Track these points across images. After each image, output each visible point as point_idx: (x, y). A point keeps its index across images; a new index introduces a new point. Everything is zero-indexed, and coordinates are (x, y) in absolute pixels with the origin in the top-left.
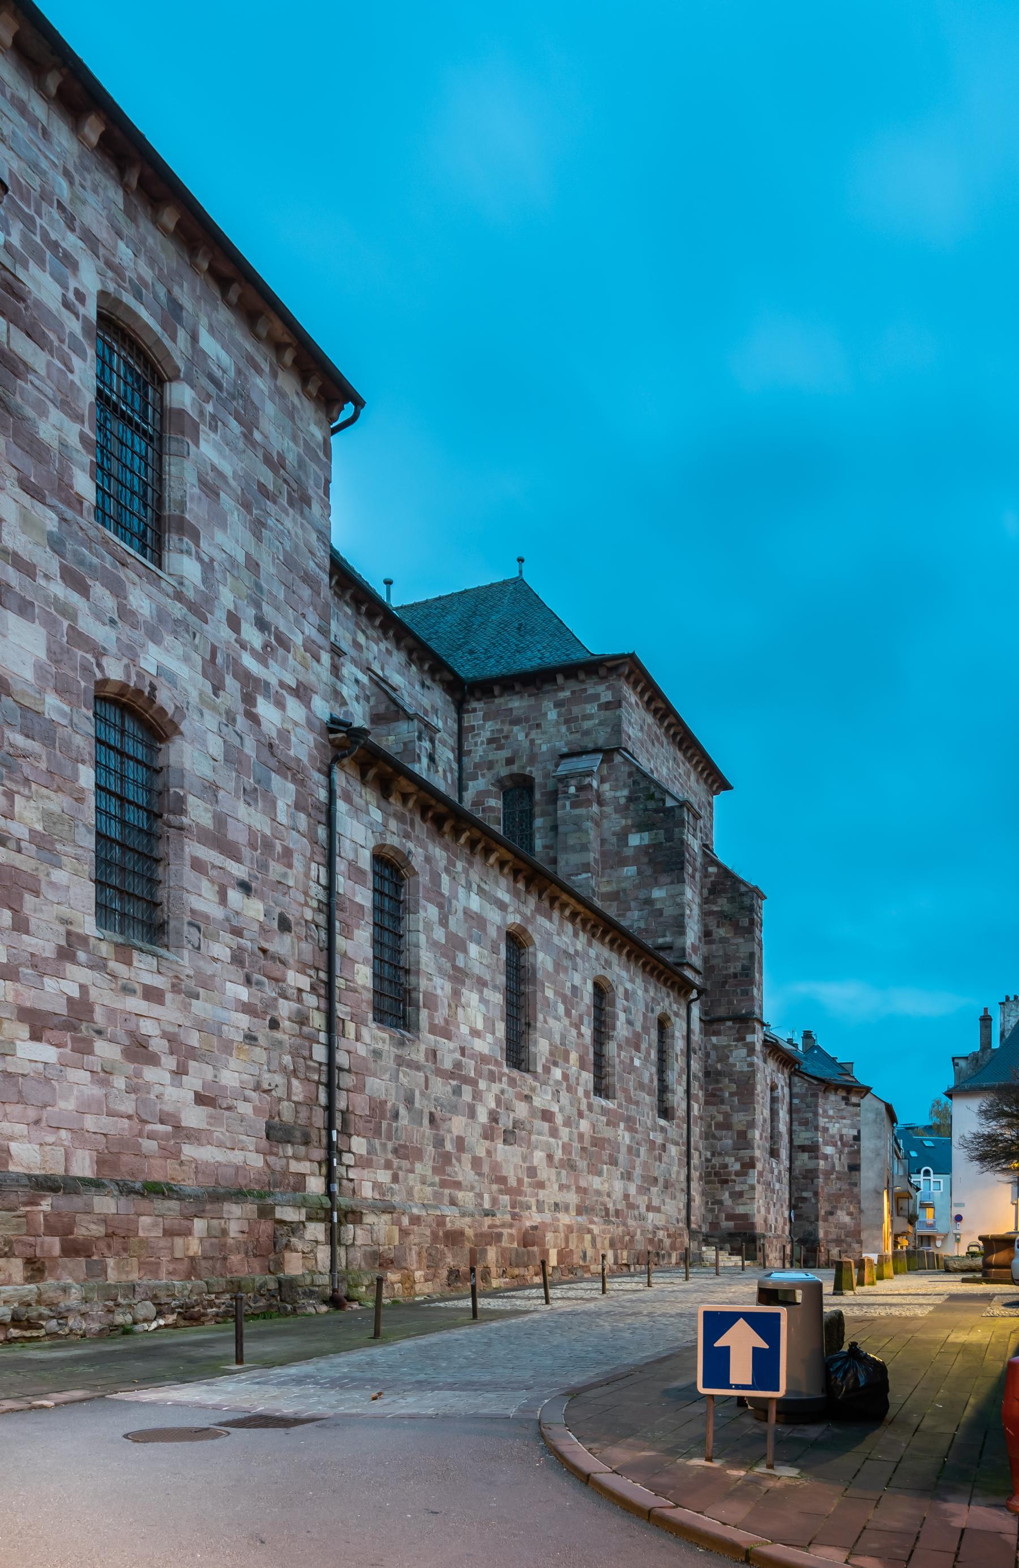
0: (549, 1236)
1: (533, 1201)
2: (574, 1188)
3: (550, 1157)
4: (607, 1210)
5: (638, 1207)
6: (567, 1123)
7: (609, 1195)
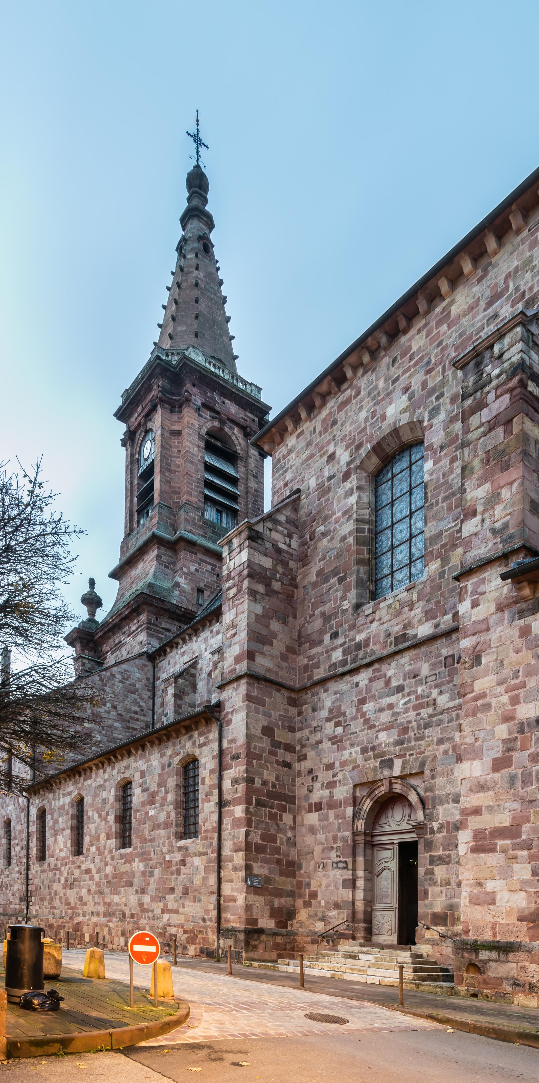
0: (85, 927)
1: (81, 912)
2: (102, 904)
3: (89, 890)
4: (124, 915)
5: (152, 911)
6: (99, 871)
7: (126, 905)
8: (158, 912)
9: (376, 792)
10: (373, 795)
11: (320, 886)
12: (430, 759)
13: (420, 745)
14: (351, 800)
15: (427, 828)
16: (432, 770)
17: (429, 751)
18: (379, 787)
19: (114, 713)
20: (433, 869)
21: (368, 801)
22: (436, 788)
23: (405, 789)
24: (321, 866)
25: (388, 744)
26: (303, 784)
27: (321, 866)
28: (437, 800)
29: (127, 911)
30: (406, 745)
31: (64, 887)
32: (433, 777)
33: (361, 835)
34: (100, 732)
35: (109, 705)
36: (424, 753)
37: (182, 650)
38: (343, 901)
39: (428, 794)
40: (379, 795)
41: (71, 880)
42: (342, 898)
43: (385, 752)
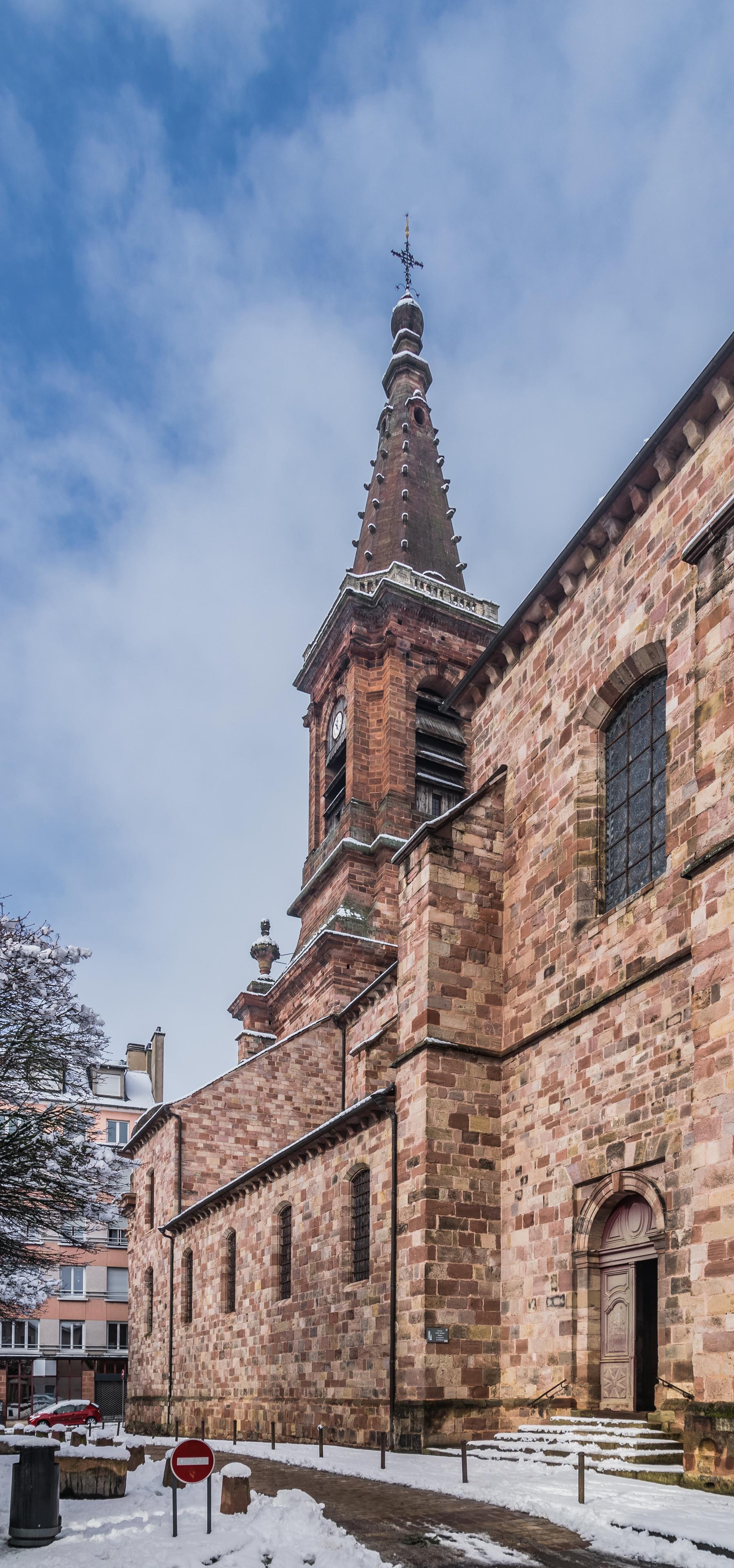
0: (236, 1411)
2: (256, 1377)
3: (242, 1360)
6: (253, 1333)
7: (284, 1378)
8: (321, 1385)
9: (603, 1192)
10: (599, 1197)
11: (531, 1333)
12: (673, 1138)
13: (660, 1119)
14: (571, 1207)
15: (668, 1240)
16: (675, 1154)
17: (671, 1127)
18: (607, 1185)
19: (288, 1107)
20: (676, 1299)
21: (593, 1205)
22: (680, 1180)
23: (641, 1184)
24: (533, 1305)
25: (618, 1122)
26: (509, 1189)
27: (533, 1305)
28: (682, 1198)
29: (285, 1386)
30: (641, 1121)
31: (213, 1358)
32: (677, 1164)
33: (583, 1256)
34: (269, 1136)
35: (281, 1097)
36: (664, 1130)
37: (380, 1007)
38: (560, 1354)
39: (670, 1189)
40: (607, 1196)
41: (220, 1347)
42: (559, 1348)
43: (614, 1134)
